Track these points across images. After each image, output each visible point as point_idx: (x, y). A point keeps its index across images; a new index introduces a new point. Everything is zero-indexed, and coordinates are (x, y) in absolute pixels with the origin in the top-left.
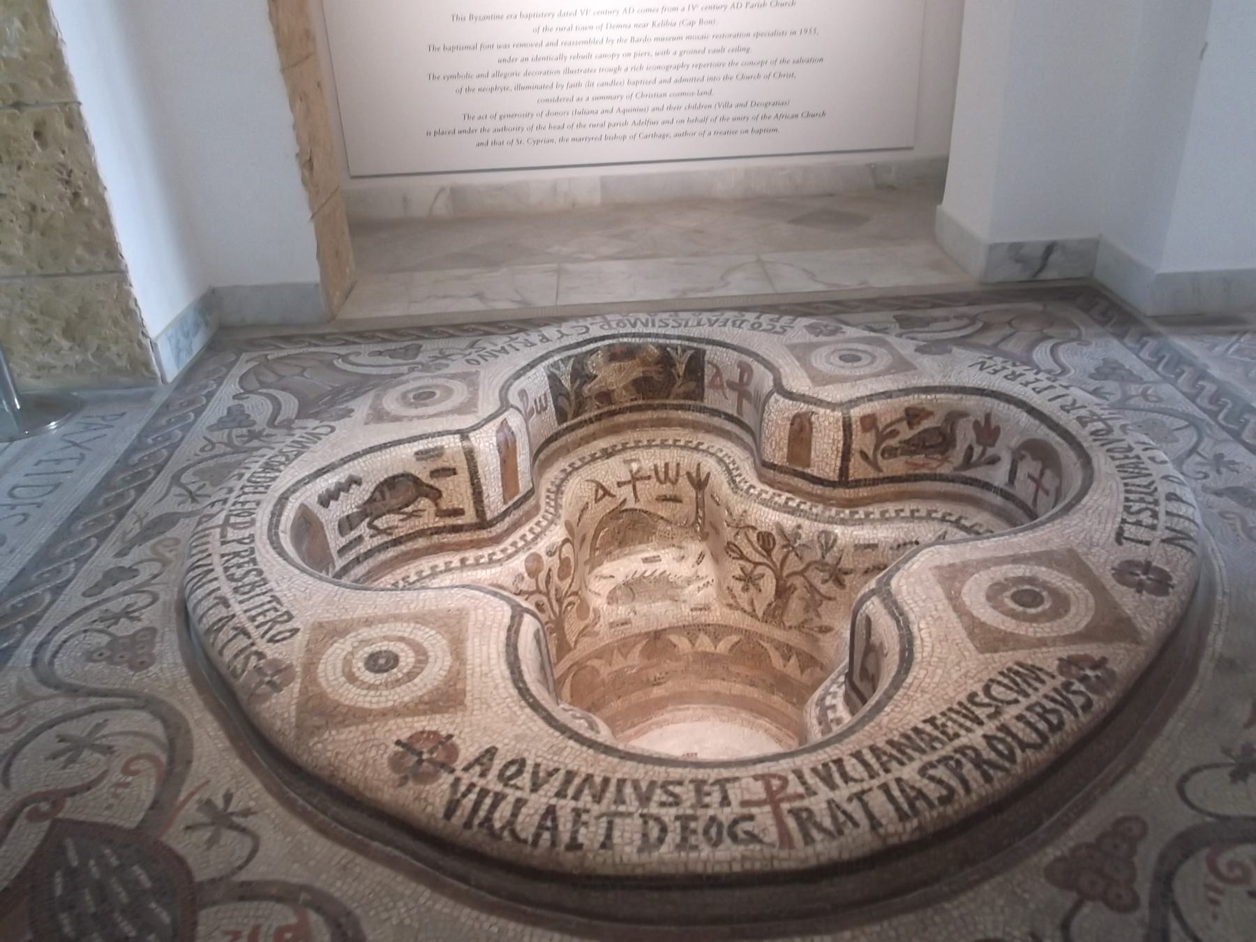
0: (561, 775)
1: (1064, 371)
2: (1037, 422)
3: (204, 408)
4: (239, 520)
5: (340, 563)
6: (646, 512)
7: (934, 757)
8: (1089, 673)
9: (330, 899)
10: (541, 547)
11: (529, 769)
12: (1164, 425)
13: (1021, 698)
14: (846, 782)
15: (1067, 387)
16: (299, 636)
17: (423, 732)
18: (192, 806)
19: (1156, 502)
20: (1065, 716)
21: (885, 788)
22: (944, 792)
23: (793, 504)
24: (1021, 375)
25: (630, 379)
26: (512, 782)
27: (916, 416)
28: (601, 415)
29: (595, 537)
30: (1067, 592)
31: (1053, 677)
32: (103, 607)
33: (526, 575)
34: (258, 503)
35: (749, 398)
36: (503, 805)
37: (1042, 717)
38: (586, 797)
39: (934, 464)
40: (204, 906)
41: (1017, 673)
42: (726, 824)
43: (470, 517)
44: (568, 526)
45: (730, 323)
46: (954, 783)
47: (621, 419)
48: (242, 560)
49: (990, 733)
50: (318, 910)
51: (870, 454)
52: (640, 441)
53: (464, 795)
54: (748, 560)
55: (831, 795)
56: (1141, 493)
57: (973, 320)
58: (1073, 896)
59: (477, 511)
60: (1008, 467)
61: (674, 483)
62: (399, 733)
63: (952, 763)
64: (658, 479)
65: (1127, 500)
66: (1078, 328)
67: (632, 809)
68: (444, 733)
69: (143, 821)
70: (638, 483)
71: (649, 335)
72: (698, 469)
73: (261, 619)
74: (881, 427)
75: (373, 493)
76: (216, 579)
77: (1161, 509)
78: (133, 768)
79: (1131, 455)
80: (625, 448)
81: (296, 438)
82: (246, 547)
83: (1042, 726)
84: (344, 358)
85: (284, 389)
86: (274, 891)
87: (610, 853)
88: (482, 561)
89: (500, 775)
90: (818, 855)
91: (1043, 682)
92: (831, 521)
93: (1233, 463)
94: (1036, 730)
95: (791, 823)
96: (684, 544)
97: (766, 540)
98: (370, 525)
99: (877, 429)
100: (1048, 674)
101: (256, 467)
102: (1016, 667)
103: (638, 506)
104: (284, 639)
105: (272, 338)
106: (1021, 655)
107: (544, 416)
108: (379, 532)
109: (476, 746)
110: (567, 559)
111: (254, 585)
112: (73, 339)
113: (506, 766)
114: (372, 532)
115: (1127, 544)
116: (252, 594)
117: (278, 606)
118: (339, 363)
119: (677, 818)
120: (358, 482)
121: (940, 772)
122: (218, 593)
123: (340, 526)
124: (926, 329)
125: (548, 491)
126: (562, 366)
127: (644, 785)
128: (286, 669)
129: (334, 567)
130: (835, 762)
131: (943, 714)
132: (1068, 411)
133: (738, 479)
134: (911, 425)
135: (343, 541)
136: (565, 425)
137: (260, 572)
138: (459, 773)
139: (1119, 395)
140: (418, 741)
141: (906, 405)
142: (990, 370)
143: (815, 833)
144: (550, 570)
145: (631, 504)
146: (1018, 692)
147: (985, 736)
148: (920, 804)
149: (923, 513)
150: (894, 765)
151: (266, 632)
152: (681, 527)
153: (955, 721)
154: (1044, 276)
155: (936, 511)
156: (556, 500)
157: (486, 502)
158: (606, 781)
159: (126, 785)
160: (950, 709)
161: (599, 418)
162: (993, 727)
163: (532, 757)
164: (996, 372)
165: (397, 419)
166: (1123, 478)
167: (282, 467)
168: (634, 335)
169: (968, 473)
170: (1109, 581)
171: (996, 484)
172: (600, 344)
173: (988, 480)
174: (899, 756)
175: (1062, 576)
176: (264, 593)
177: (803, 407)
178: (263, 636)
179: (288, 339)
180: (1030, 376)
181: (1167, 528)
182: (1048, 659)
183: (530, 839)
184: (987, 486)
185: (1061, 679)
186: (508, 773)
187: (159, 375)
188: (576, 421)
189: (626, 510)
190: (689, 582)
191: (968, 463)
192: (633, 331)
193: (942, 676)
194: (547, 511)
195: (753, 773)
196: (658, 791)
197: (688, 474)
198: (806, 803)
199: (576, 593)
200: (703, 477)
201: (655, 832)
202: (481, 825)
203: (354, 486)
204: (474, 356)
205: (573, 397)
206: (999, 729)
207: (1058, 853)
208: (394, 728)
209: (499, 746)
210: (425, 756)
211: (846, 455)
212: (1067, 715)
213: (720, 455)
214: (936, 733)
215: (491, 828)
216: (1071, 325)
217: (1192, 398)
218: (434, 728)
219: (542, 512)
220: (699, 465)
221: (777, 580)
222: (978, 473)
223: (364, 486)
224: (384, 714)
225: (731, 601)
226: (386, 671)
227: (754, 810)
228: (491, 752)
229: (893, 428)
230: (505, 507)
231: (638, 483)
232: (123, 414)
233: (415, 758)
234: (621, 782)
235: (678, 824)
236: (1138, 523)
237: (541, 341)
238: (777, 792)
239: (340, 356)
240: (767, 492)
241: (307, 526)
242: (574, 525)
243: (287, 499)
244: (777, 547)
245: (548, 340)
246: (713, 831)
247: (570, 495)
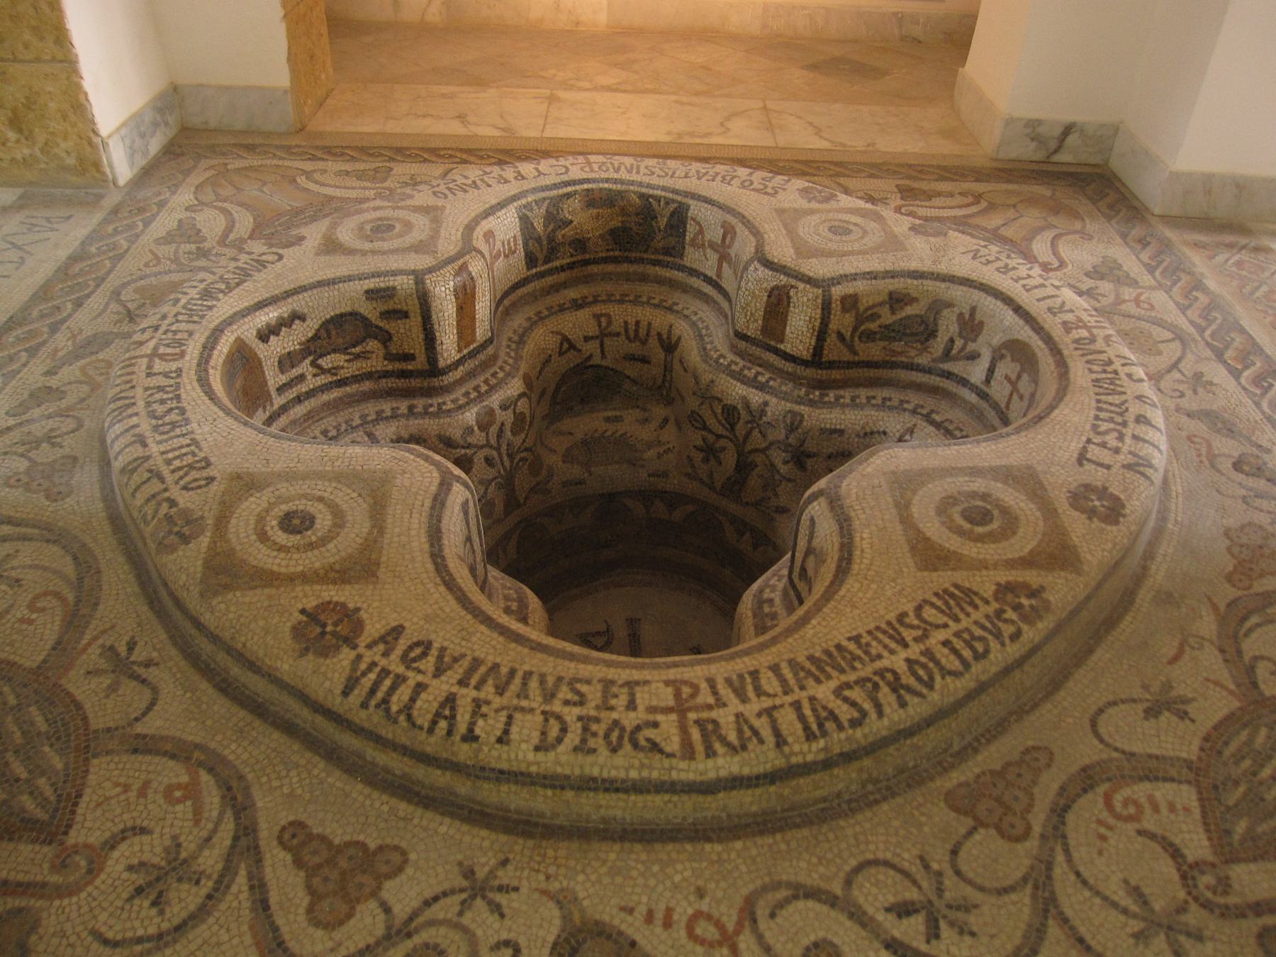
0: (465, 663)
1: (1062, 264)
2: (1021, 322)
3: (154, 216)
4: (169, 350)
5: (278, 401)
7: (852, 677)
8: (1025, 601)
9: (223, 760)
10: (495, 400)
11: (434, 652)
12: (1150, 335)
13: (951, 623)
14: (758, 696)
15: (1057, 288)
16: (214, 487)
17: (329, 603)
18: (94, 651)
19: (1124, 424)
20: (992, 644)
21: (797, 706)
22: (856, 715)
23: (762, 379)
24: (1014, 268)
25: (608, 228)
26: (415, 665)
27: (898, 301)
28: (574, 263)
29: (557, 390)
30: (1018, 512)
31: (987, 602)
32: (26, 429)
34: (191, 334)
35: (729, 262)
36: (402, 688)
37: (969, 644)
38: (489, 689)
39: (913, 353)
40: (95, 756)
41: (952, 595)
42: (628, 730)
43: (420, 362)
44: (527, 380)
45: (719, 178)
46: (867, 706)
47: (594, 269)
48: (165, 396)
49: (913, 657)
50: (211, 770)
51: (848, 335)
53: (364, 674)
54: (710, 431)
55: (741, 708)
56: (1112, 412)
57: (978, 198)
58: (970, 822)
59: (428, 358)
60: (987, 365)
61: (644, 342)
62: (304, 600)
63: (869, 685)
64: (628, 338)
65: (1097, 418)
66: (1083, 220)
67: (535, 705)
68: (351, 606)
69: (44, 661)
71: (632, 183)
73: (177, 463)
74: (862, 309)
75: (318, 330)
76: (137, 414)
77: (1128, 432)
78: (38, 605)
79: (1109, 369)
80: (596, 301)
81: (240, 264)
82: (172, 382)
83: (967, 653)
84: (308, 175)
85: (241, 205)
86: (168, 747)
87: (505, 748)
88: (431, 409)
89: (404, 658)
90: (718, 769)
91: (976, 607)
92: (799, 401)
93: (1211, 383)
95: (696, 734)
96: (649, 407)
97: (730, 413)
98: (313, 364)
99: (857, 309)
100: (983, 599)
101: (193, 293)
102: (952, 589)
103: (604, 363)
104: (200, 487)
105: (235, 145)
106: (961, 577)
107: (512, 260)
108: (323, 371)
109: (384, 622)
110: (521, 413)
111: (174, 425)
112: (20, 131)
113: (411, 648)
114: (315, 371)
115: (1088, 466)
116: (172, 434)
117: (197, 451)
118: (302, 180)
119: (580, 718)
120: (302, 318)
121: (856, 694)
122: (137, 431)
123: (280, 362)
124: (927, 204)
125: (510, 339)
127: (551, 680)
128: (197, 520)
129: (272, 405)
130: (751, 673)
131: (869, 632)
132: (1054, 314)
133: (709, 347)
134: (893, 312)
135: (283, 379)
136: (534, 271)
137: (183, 411)
138: (361, 650)
139: (1111, 298)
140: (323, 612)
141: (891, 288)
142: (983, 260)
143: (717, 746)
144: (503, 424)
145: (597, 360)
146: (949, 616)
147: (908, 660)
148: (830, 726)
149: (895, 403)
150: (810, 682)
151: (181, 478)
153: (880, 642)
154: (1056, 158)
155: (908, 402)
156: (516, 351)
157: (439, 348)
158: (512, 672)
159: (31, 622)
160: (878, 628)
161: (571, 266)
162: (918, 650)
163: (439, 640)
164: (989, 262)
165: (351, 252)
166: (1097, 394)
167: (221, 296)
168: (615, 181)
169: (946, 366)
170: (1062, 503)
171: (973, 380)
172: (578, 187)
173: (964, 375)
174: (817, 673)
175: (1016, 494)
176: (183, 435)
177: (783, 279)
178: (177, 483)
179: (251, 148)
180: (1023, 271)
181: (1130, 453)
182: (985, 584)
183: (426, 725)
184: (964, 382)
185: (995, 605)
186: (412, 655)
187: (110, 176)
188: (546, 267)
190: (650, 445)
191: (947, 355)
192: (616, 176)
193: (876, 592)
194: (505, 362)
195: (664, 678)
196: (564, 688)
198: (714, 714)
199: (526, 450)
201: (554, 731)
202: (378, 706)
203: (297, 322)
204: (442, 188)
205: (545, 242)
206: (922, 653)
207: (962, 779)
208: (301, 595)
209: (407, 625)
210: (329, 629)
211: (821, 335)
212: (994, 645)
213: (694, 318)
214: (859, 652)
215: (388, 710)
216: (1076, 215)
217: (1183, 309)
218: (342, 599)
219: (500, 363)
221: (739, 456)
222: (956, 367)
223: (308, 322)
224: (291, 579)
225: (690, 471)
226: (300, 532)
227: (660, 718)
228: (398, 631)
229: (875, 310)
230: (459, 356)
232: (70, 217)
233: (318, 630)
234: (528, 675)
235: (579, 724)
236: (1103, 445)
237: (516, 178)
238: (687, 700)
239: (304, 172)
240: (736, 364)
241: (242, 360)
243: (222, 331)
244: (742, 421)
245: (523, 178)
246: (614, 736)
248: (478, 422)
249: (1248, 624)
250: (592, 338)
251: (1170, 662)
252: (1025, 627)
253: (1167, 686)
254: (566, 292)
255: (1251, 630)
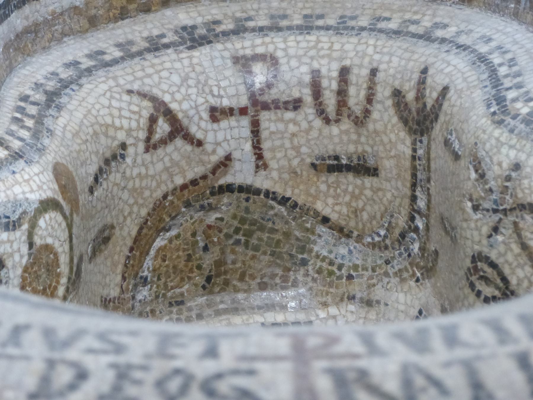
6: (284, 201)
52: (285, 17)
55: (413, 357)
64: (321, 112)
70: (265, 116)
72: (422, 82)
96: (378, 293)
110: (47, 248)
119: (113, 366)
125: (25, 98)
133: (511, 95)
152: (373, 245)
156: (39, 120)
189: (229, 188)
197: (397, 94)
198: (362, 363)
200: (430, 100)
213: (483, 49)
220: (425, 71)
231: (265, 116)
242: (82, 186)
246: (174, 385)
247: (79, 115)
250: (230, 112)
254: (168, 12)
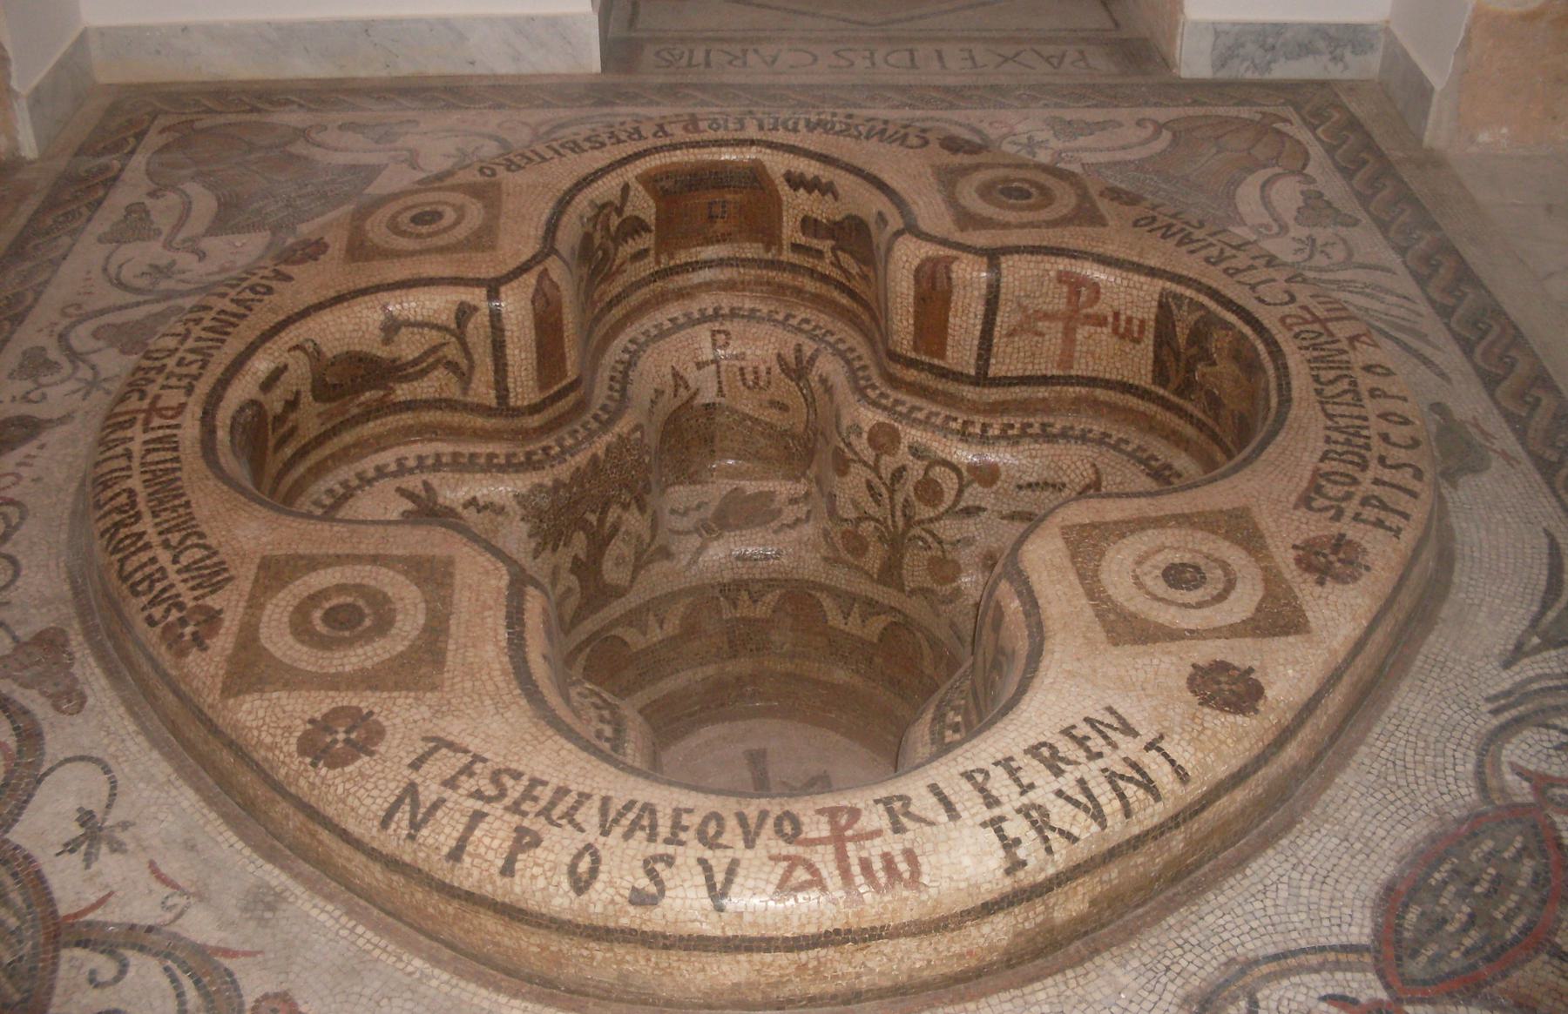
8: (189, 630)
33: (865, 436)
83: (138, 576)
91: (193, 588)
94: (136, 571)
120: (836, 197)
126: (1185, 308)
248: (871, 432)
249: (187, 983)
251: (152, 864)
252: (158, 629)
253: (117, 847)
255: (174, 980)
